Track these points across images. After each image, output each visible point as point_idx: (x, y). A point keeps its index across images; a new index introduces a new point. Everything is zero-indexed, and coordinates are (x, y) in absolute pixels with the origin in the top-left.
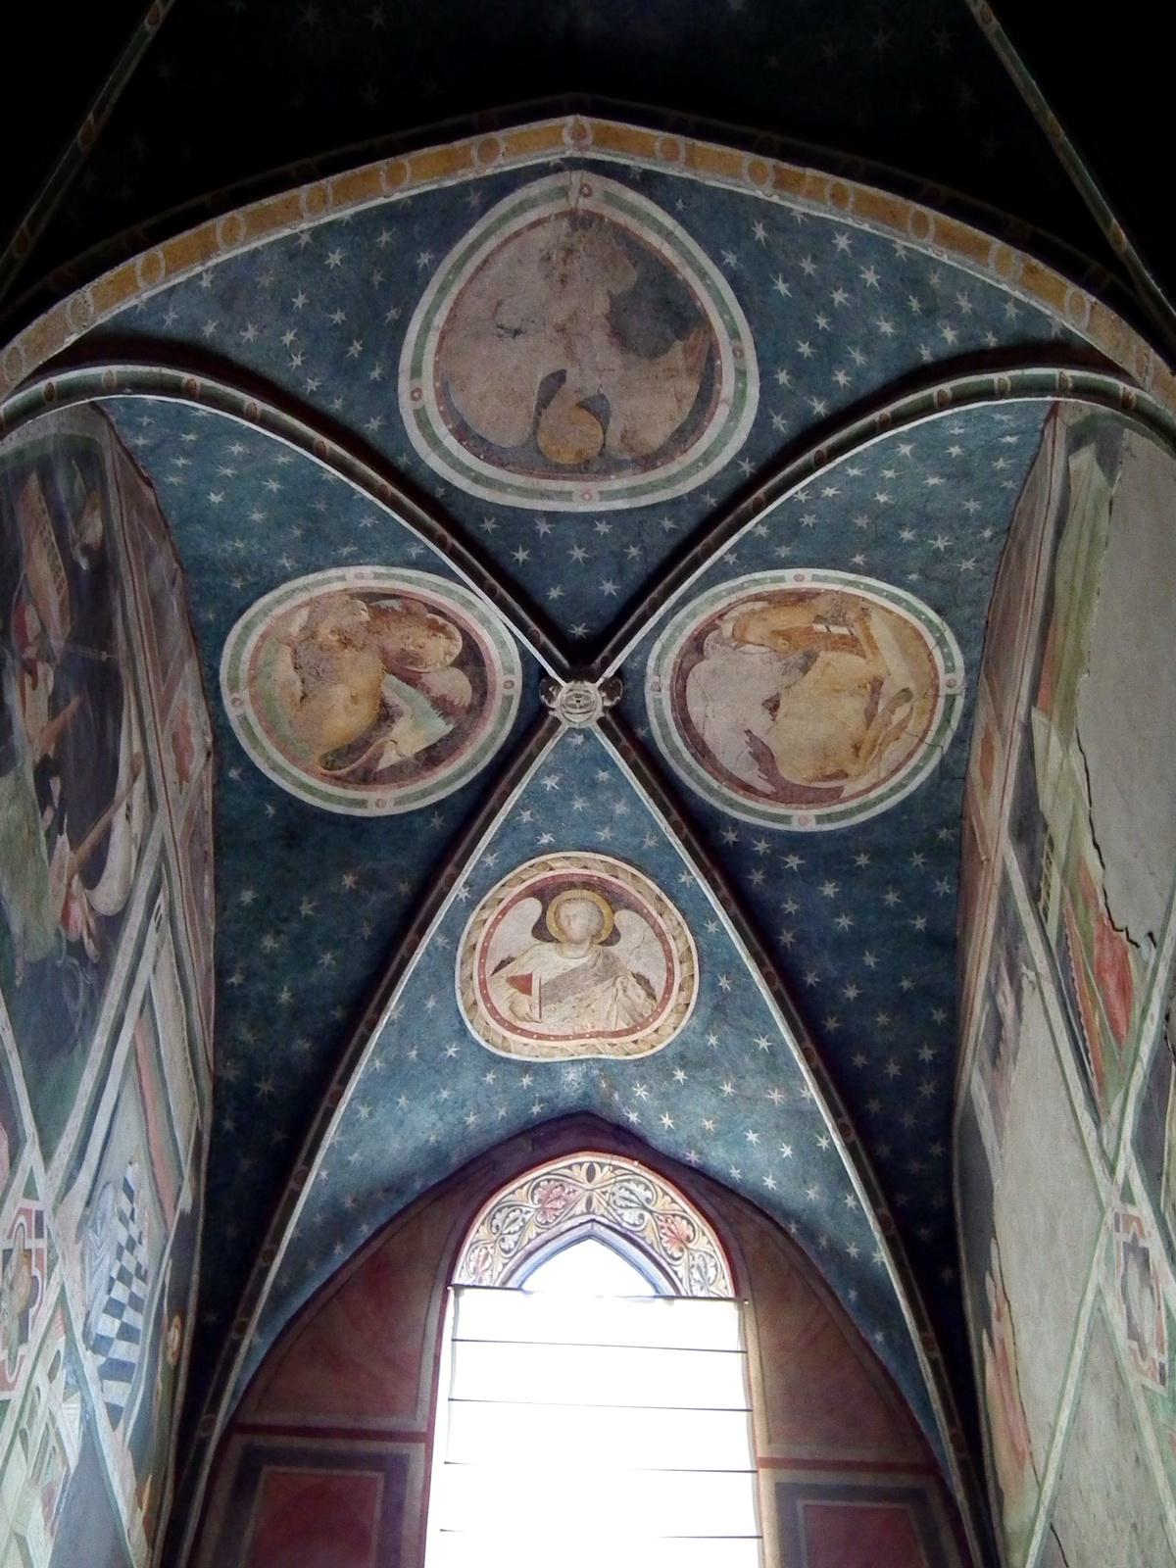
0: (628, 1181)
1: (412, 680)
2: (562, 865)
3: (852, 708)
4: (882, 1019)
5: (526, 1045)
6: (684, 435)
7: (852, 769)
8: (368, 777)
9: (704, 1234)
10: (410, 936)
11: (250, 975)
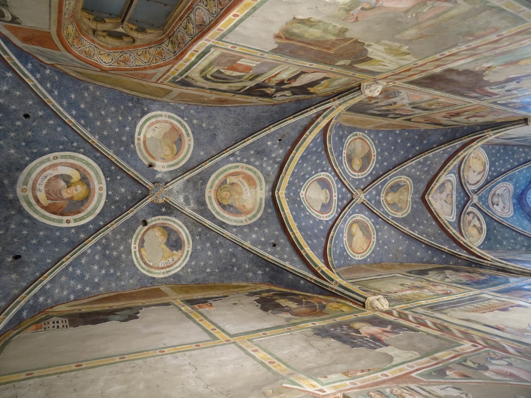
1: (471, 222)
2: (490, 202)
3: (475, 161)
4: (516, 156)
6: (452, 184)
8: (482, 229)
11: (509, 246)
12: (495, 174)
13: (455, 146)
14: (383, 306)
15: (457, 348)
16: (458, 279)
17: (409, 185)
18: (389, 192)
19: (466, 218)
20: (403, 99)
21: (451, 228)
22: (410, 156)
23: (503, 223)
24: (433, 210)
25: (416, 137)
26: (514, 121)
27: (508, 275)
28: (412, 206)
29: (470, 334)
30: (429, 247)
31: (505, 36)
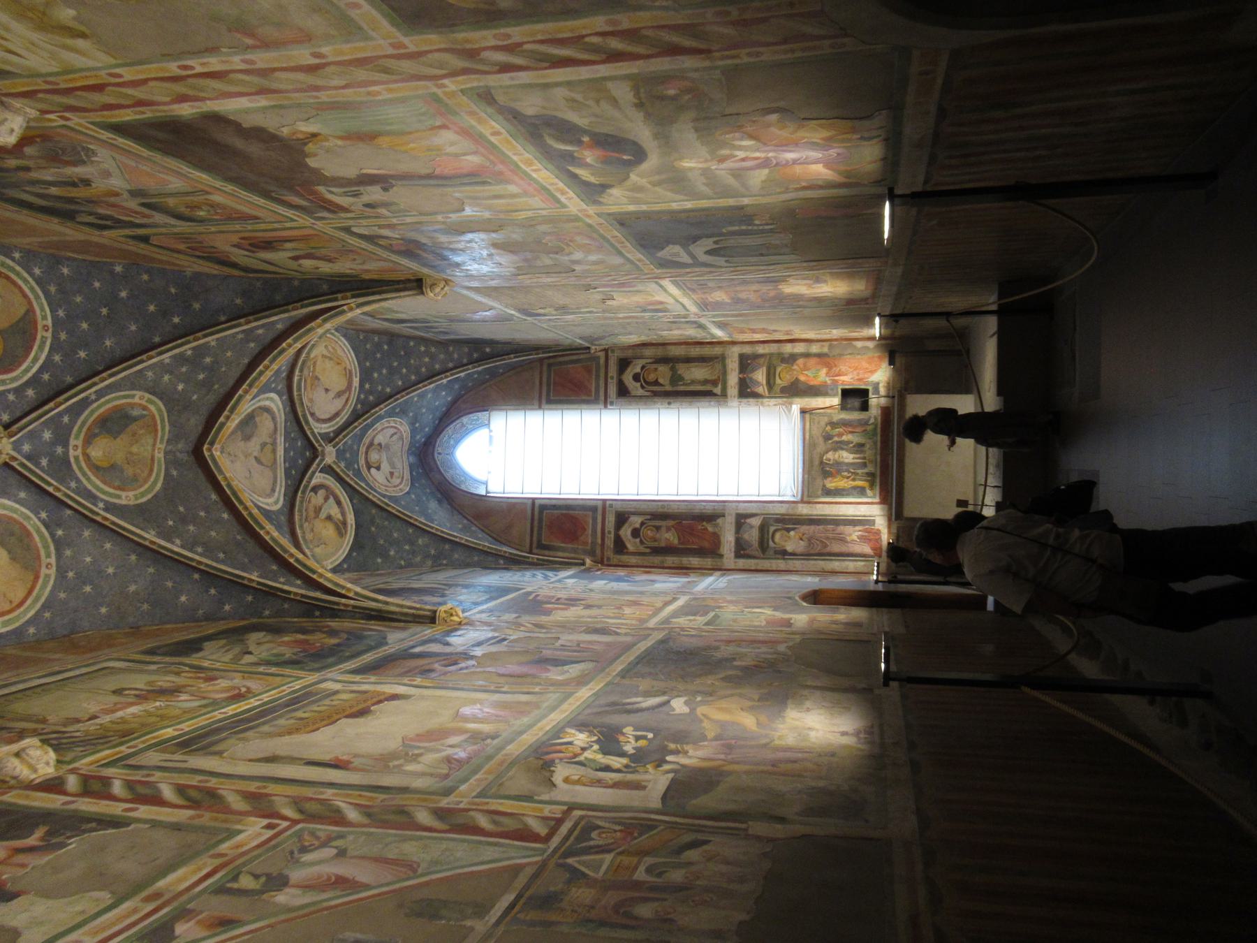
2: (362, 462)
3: (329, 364)
4: (412, 362)
6: (274, 419)
7: (344, 365)
8: (344, 523)
11: (402, 558)
12: (371, 398)
13: (273, 323)
14: (35, 771)
15: (224, 847)
16: (274, 651)
17: (157, 417)
18: (95, 435)
19: (309, 502)
20: (107, 174)
21: (269, 527)
22: (157, 339)
23: (389, 509)
24: (223, 484)
25: (173, 290)
26: (398, 282)
27: (386, 626)
28: (167, 474)
29: (267, 795)
30: (210, 577)
31: (330, 59)
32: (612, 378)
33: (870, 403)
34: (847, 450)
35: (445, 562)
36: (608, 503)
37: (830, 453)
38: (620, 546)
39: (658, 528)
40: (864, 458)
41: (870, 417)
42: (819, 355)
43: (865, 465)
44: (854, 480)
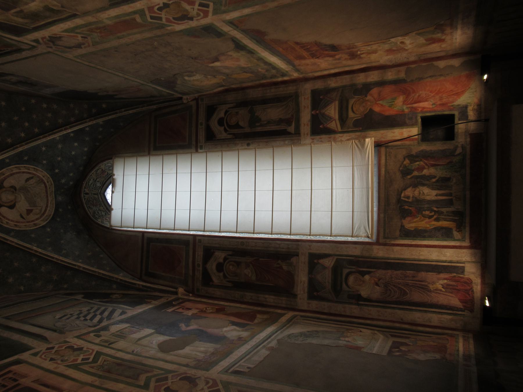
0: (89, 185)
5: (49, 210)
9: (100, 166)
10: (9, 242)
32: (201, 124)
33: (456, 130)
34: (428, 186)
35: (65, 286)
36: (198, 238)
37: (409, 189)
38: (207, 279)
39: (238, 264)
40: (450, 194)
41: (456, 148)
42: (395, 82)
43: (450, 203)
44: (437, 220)
